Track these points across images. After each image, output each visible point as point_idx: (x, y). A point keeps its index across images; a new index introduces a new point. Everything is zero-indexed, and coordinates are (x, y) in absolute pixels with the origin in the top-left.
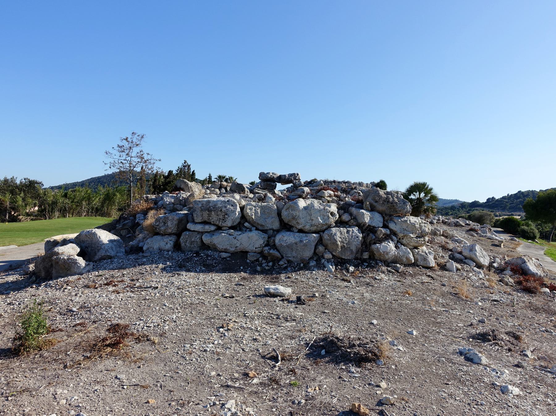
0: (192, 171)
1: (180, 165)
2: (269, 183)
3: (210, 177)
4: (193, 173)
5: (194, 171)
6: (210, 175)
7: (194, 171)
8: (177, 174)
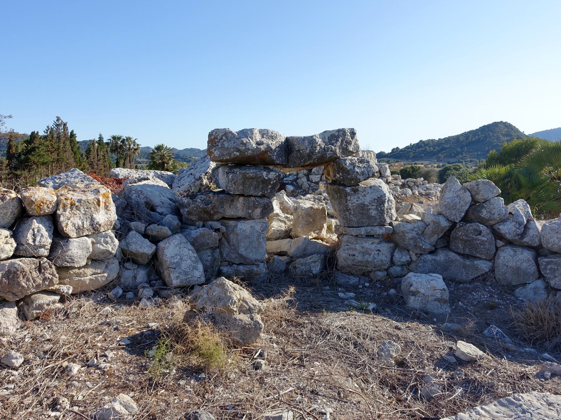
1: (51, 125)
2: (251, 172)
3: (101, 138)
4: (72, 135)
5: (72, 131)
6: (100, 135)
7: (72, 131)
8: (45, 137)
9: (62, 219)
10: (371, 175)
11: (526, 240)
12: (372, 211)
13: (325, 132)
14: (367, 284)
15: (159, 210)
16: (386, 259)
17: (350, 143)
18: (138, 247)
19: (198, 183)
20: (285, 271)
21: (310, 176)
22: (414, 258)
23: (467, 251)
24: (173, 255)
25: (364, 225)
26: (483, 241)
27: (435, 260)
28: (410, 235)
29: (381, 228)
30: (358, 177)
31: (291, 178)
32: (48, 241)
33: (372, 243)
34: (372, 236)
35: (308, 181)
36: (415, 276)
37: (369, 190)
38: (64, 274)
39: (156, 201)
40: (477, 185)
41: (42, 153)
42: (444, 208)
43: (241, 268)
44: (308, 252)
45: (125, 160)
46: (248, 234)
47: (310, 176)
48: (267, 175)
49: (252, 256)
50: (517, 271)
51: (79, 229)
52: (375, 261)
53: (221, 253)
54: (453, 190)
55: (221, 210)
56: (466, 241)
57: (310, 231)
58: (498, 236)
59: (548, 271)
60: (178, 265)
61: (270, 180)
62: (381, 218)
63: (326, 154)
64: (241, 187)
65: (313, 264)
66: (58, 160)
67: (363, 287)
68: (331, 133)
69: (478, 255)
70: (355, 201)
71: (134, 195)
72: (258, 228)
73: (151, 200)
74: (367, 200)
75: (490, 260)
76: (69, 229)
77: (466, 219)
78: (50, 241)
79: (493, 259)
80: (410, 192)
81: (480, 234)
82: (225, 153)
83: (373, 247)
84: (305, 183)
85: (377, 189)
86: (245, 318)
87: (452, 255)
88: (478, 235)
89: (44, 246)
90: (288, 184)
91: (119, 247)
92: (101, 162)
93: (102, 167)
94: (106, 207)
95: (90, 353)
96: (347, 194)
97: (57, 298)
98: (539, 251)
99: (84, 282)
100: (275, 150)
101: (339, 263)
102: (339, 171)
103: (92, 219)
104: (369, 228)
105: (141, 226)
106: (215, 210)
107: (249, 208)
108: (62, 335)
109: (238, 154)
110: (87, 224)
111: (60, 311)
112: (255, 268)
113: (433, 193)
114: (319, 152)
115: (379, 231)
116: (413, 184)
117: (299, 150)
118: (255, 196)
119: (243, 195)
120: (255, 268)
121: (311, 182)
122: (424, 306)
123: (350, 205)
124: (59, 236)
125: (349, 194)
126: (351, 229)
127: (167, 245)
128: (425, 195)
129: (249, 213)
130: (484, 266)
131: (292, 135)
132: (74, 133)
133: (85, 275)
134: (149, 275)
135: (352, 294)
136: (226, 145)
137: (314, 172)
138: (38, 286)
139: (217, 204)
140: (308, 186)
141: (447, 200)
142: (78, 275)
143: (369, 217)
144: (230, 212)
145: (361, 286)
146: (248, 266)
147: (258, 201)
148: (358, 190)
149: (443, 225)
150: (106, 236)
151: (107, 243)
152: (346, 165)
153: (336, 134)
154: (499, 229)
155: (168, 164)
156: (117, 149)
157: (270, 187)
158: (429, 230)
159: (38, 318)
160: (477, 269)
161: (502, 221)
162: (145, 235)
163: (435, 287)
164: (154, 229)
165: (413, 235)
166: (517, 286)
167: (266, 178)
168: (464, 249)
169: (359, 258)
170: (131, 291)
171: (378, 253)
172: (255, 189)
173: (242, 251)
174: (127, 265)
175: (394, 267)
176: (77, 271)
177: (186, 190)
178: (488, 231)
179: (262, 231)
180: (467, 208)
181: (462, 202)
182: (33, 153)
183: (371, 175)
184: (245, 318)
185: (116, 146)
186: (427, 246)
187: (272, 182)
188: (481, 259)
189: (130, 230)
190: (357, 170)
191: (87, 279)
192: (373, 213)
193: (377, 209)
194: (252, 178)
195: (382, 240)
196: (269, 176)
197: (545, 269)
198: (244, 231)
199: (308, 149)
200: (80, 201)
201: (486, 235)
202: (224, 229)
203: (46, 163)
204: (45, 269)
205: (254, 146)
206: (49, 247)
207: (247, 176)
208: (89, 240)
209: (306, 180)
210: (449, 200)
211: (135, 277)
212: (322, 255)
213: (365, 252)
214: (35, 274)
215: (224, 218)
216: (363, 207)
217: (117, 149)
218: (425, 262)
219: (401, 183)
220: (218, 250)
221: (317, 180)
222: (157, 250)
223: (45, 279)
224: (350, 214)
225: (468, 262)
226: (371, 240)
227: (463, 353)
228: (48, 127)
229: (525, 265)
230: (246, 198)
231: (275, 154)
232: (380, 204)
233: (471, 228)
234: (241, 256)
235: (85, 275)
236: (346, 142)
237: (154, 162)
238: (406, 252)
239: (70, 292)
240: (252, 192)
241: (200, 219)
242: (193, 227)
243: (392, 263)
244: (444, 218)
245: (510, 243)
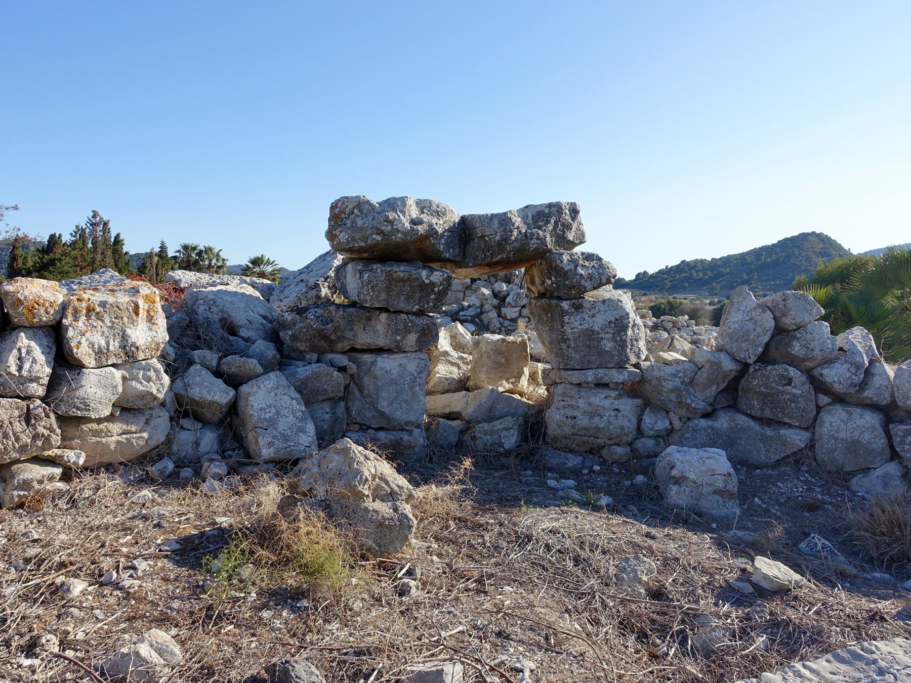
0: (113, 235)
2: (401, 270)
3: (163, 248)
4: (118, 241)
5: (118, 235)
6: (163, 243)
7: (118, 235)
8: (74, 243)
9: (70, 333)
10: (604, 281)
11: (868, 393)
12: (605, 342)
13: (527, 207)
14: (597, 468)
15: (244, 333)
16: (629, 424)
17: (568, 227)
18: (204, 391)
19: (313, 293)
20: (457, 444)
21: (503, 309)
22: (677, 424)
23: (768, 413)
24: (264, 406)
25: (593, 366)
26: (794, 395)
27: (713, 428)
28: (670, 385)
29: (621, 372)
30: (583, 282)
31: (471, 312)
32: (44, 370)
33: (606, 398)
34: (606, 385)
35: (499, 316)
36: (679, 452)
37: (600, 306)
38: (72, 431)
39: (240, 317)
40: (784, 300)
41: (66, 268)
42: (727, 339)
43: (381, 434)
44: (497, 413)
46: (393, 377)
47: (503, 309)
48: (428, 277)
49: (401, 415)
50: (853, 446)
51: (100, 353)
52: (611, 427)
53: (348, 409)
54: (743, 308)
55: (349, 334)
56: (765, 395)
57: (501, 378)
58: (819, 386)
59: (907, 447)
60: (272, 423)
61: (432, 284)
62: (620, 354)
63: (529, 244)
64: (383, 296)
65: (504, 433)
67: (590, 472)
68: (537, 210)
69: (786, 420)
70: (576, 324)
71: (202, 307)
72: (412, 367)
73: (230, 316)
74: (598, 323)
75: (807, 429)
76: (83, 352)
77: (764, 359)
78: (48, 370)
79: (811, 426)
81: (789, 384)
82: (358, 236)
83: (607, 403)
84: (494, 321)
85: (615, 305)
86: (383, 508)
87: (742, 419)
88: (785, 385)
89: (36, 380)
91: (171, 387)
94: (150, 319)
95: (107, 563)
96: (563, 313)
97: (58, 471)
98: (889, 412)
99: (107, 446)
100: (442, 235)
101: (550, 432)
102: (550, 274)
103: (124, 337)
104: (601, 371)
105: (212, 357)
106: (339, 334)
107: (397, 332)
108: (60, 532)
109: (379, 238)
110: (114, 345)
111: (61, 494)
112: (405, 437)
113: (704, 340)
114: (516, 240)
115: (617, 376)
116: (671, 325)
117: (483, 237)
118: (407, 313)
119: (386, 310)
120: (405, 437)
121: (505, 318)
122: (695, 502)
123: (569, 331)
124: (65, 362)
125: (567, 313)
126: (570, 372)
127: (255, 389)
129: (396, 341)
130: (797, 438)
131: (472, 213)
132: (121, 238)
133: (109, 434)
134: (221, 441)
135: (571, 482)
136: (360, 222)
137: (509, 303)
138: (23, 448)
139: (342, 323)
140: (498, 325)
141: (733, 326)
142: (96, 433)
143: (601, 353)
144: (364, 338)
145: (585, 471)
146: (394, 433)
147: (412, 321)
148: (581, 306)
149: (726, 368)
150: (147, 368)
151: (149, 380)
152: (562, 262)
153: (547, 211)
154: (821, 375)
157: (433, 297)
158: (702, 377)
159: (21, 505)
160: (785, 443)
161: (826, 363)
162: (218, 373)
163: (714, 470)
164: (233, 363)
165: (675, 384)
166: (852, 474)
167: (427, 281)
168: (762, 409)
169: (584, 422)
170: (188, 467)
171: (616, 414)
172: (407, 299)
173: (383, 406)
174: (185, 422)
175: (643, 440)
176: (94, 426)
177: (292, 305)
178: (804, 379)
179: (419, 373)
180: (766, 338)
181: (758, 329)
182: (51, 268)
183: (604, 281)
184: (383, 508)
185: (188, 261)
186: (699, 403)
187: (436, 289)
188: (790, 426)
189: (191, 363)
190: (580, 271)
191: (112, 441)
192: (608, 345)
193: (614, 339)
194: (403, 280)
195: (622, 392)
196: (432, 278)
197: (903, 442)
198: (387, 372)
199: (499, 234)
200: (103, 304)
201: (799, 386)
202: (353, 367)
204: (37, 418)
205: (407, 225)
206: (46, 381)
207: (395, 275)
208: (118, 374)
209: (496, 315)
210: (736, 326)
211: (197, 444)
212: (521, 419)
213: (594, 413)
214: (19, 427)
215: (353, 350)
216: (590, 336)
218: (695, 431)
220: (342, 404)
221: (514, 316)
222: (236, 398)
223: (36, 437)
224: (569, 347)
225: (769, 432)
226: (603, 392)
227: (766, 577)
228: (77, 227)
229: (867, 436)
230: (392, 315)
231: (443, 241)
232: (620, 331)
233: (774, 373)
234: (383, 415)
235: (109, 434)
236: (563, 225)
238: (664, 414)
239: (81, 461)
240: (402, 305)
241: (313, 349)
242: (300, 363)
243: (640, 432)
244: (728, 357)
245: (839, 399)
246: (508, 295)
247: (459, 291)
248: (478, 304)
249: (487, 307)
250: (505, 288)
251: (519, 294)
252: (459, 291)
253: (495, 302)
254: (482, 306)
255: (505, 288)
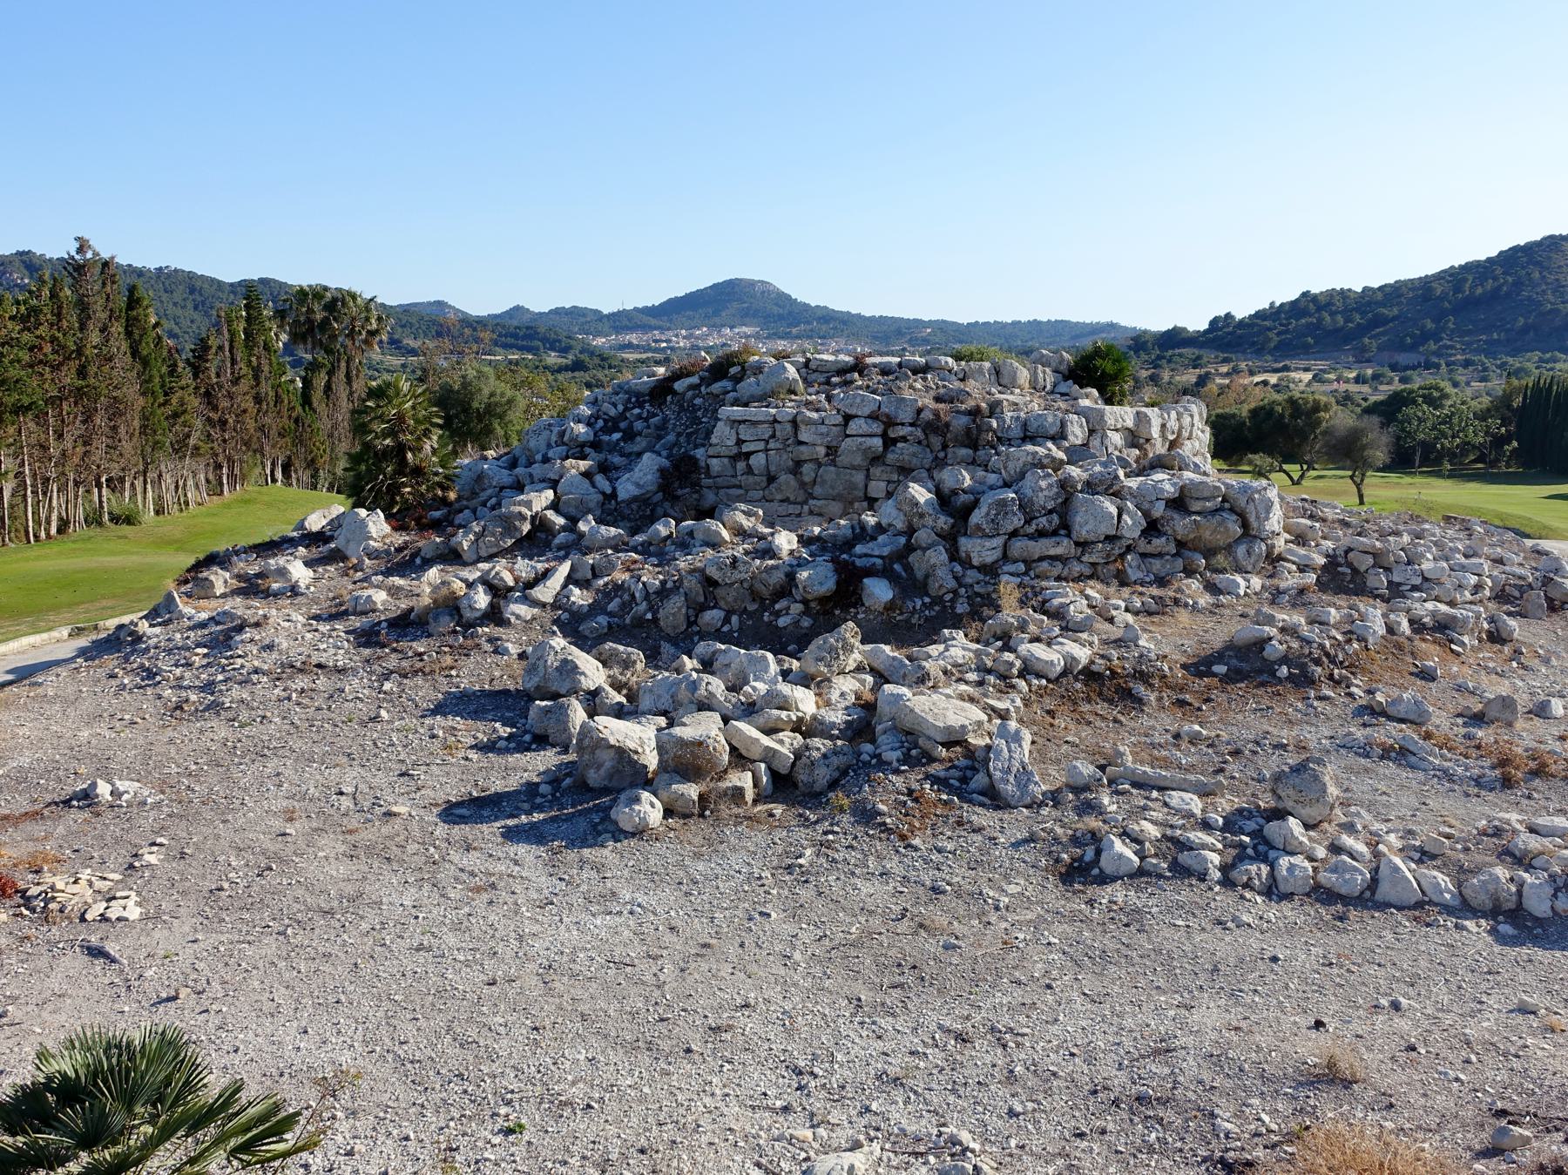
21: (963, 541)
31: (882, 547)
45: (331, 373)
47: (963, 541)
66: (79, 393)
80: (1375, 618)
84: (939, 573)
90: (870, 572)
92: (244, 385)
93: (249, 404)
113: (1465, 620)
116: (1371, 561)
121: (967, 563)
128: (1434, 629)
137: (978, 527)
140: (952, 584)
155: (417, 450)
156: (311, 330)
185: (310, 321)
203: (28, 408)
209: (944, 557)
217: (311, 330)
219: (1322, 561)
221: (990, 557)
237: (367, 446)
246: (975, 504)
247: (854, 468)
248: (900, 525)
249: (923, 536)
250: (968, 482)
251: (1003, 504)
252: (854, 468)
253: (944, 522)
254: (910, 531)
255: (968, 482)
